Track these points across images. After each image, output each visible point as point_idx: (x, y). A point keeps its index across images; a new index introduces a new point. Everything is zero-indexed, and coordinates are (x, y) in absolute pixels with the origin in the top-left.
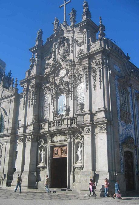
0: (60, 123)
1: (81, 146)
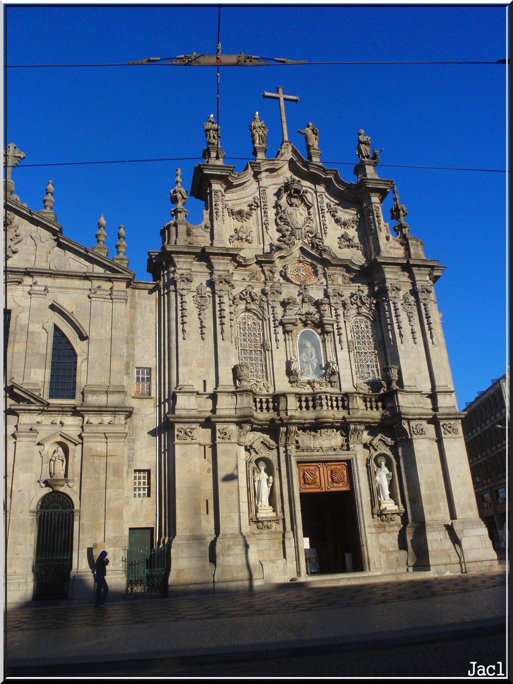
1: (389, 465)
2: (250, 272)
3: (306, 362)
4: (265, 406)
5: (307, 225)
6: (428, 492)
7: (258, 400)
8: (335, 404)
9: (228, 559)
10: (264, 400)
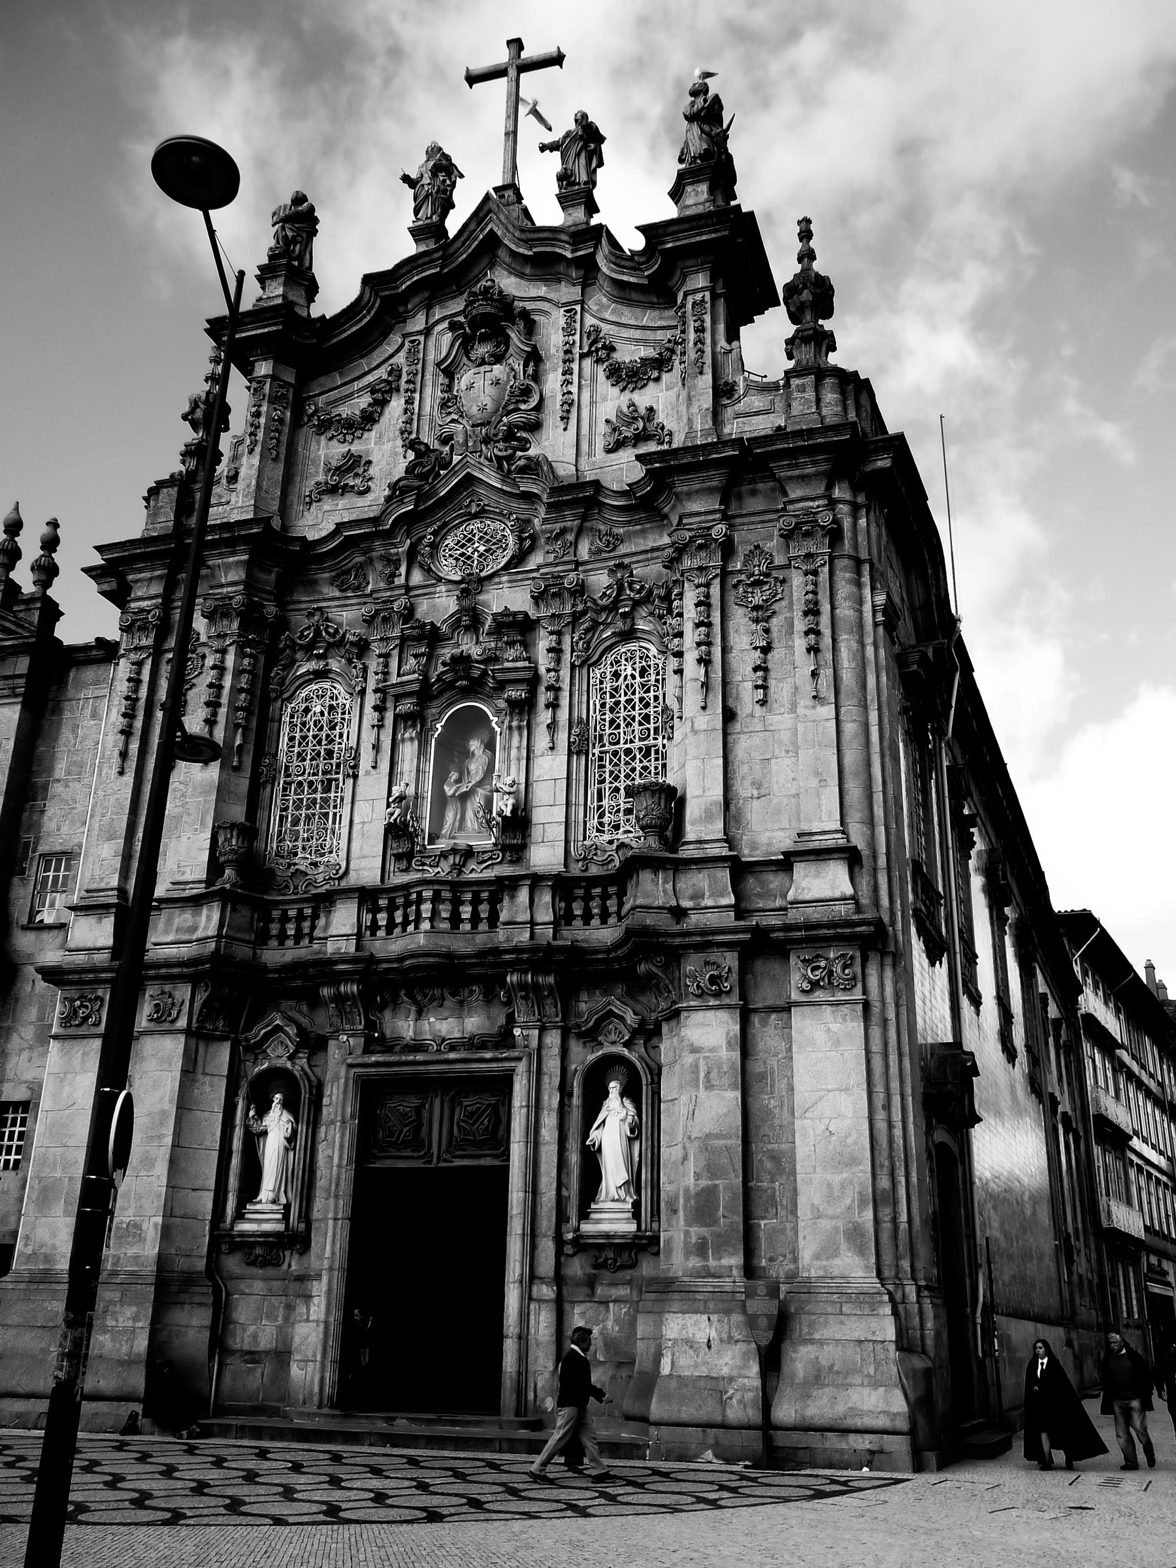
0: (466, 911)
1: (631, 1092)
2: (333, 574)
3: (453, 796)
4: (291, 930)
5: (512, 407)
6: (704, 1183)
7: (276, 914)
8: (466, 911)
9: (101, 1338)
10: (292, 913)
